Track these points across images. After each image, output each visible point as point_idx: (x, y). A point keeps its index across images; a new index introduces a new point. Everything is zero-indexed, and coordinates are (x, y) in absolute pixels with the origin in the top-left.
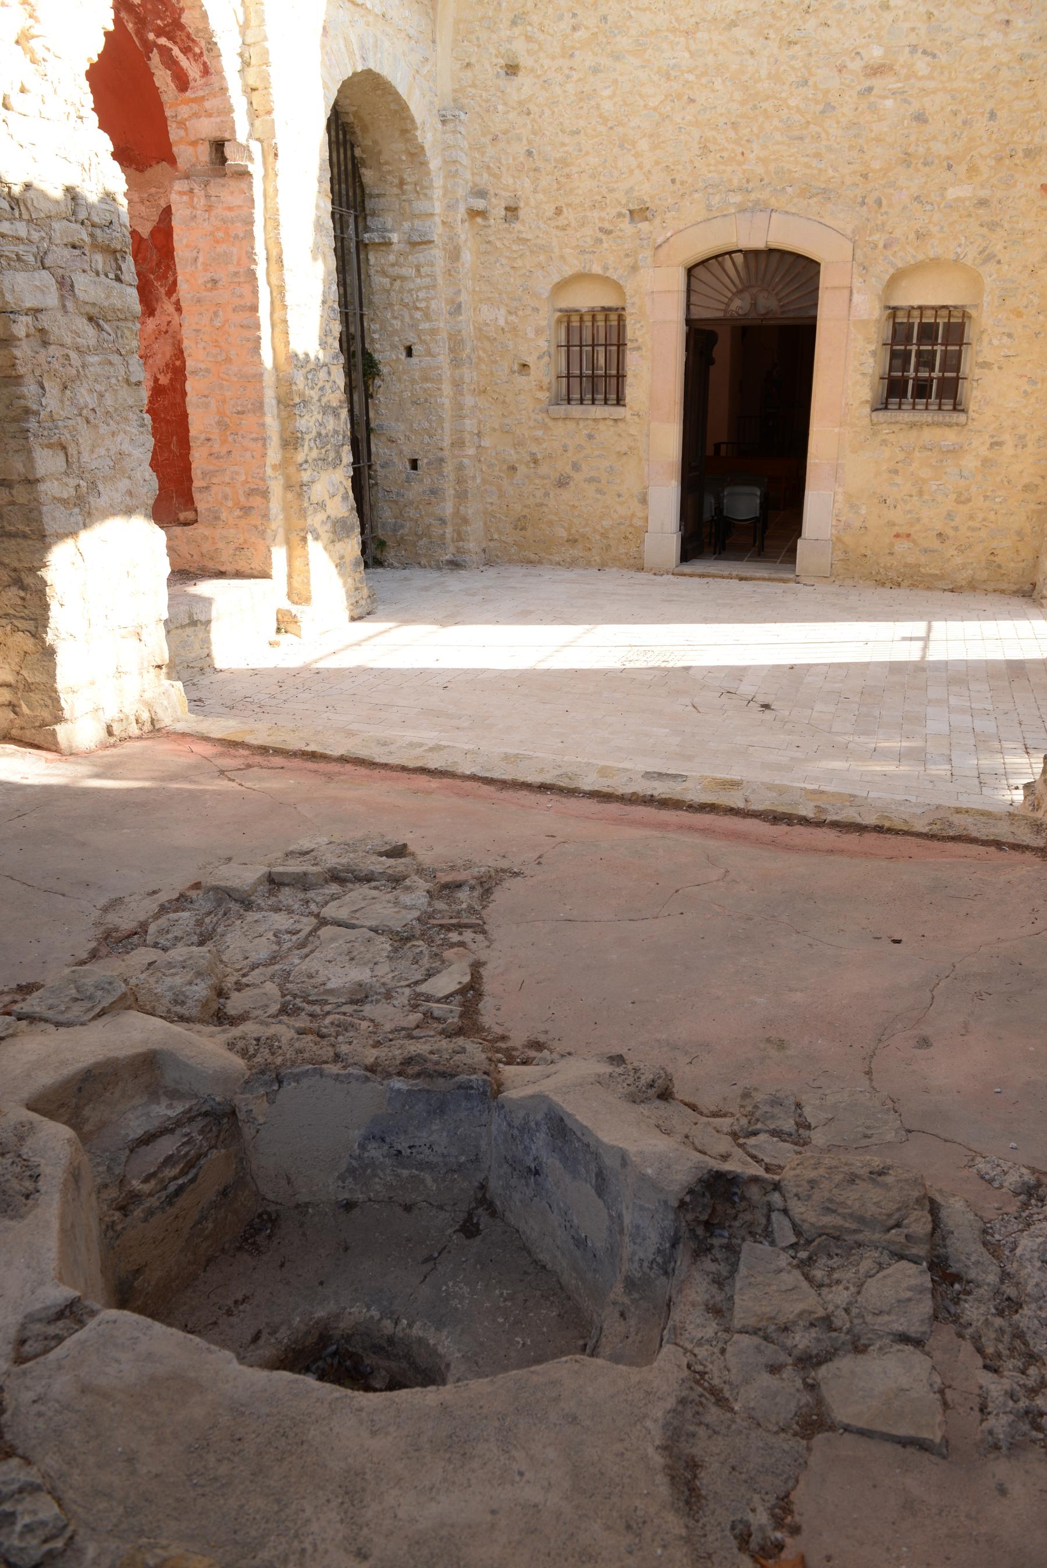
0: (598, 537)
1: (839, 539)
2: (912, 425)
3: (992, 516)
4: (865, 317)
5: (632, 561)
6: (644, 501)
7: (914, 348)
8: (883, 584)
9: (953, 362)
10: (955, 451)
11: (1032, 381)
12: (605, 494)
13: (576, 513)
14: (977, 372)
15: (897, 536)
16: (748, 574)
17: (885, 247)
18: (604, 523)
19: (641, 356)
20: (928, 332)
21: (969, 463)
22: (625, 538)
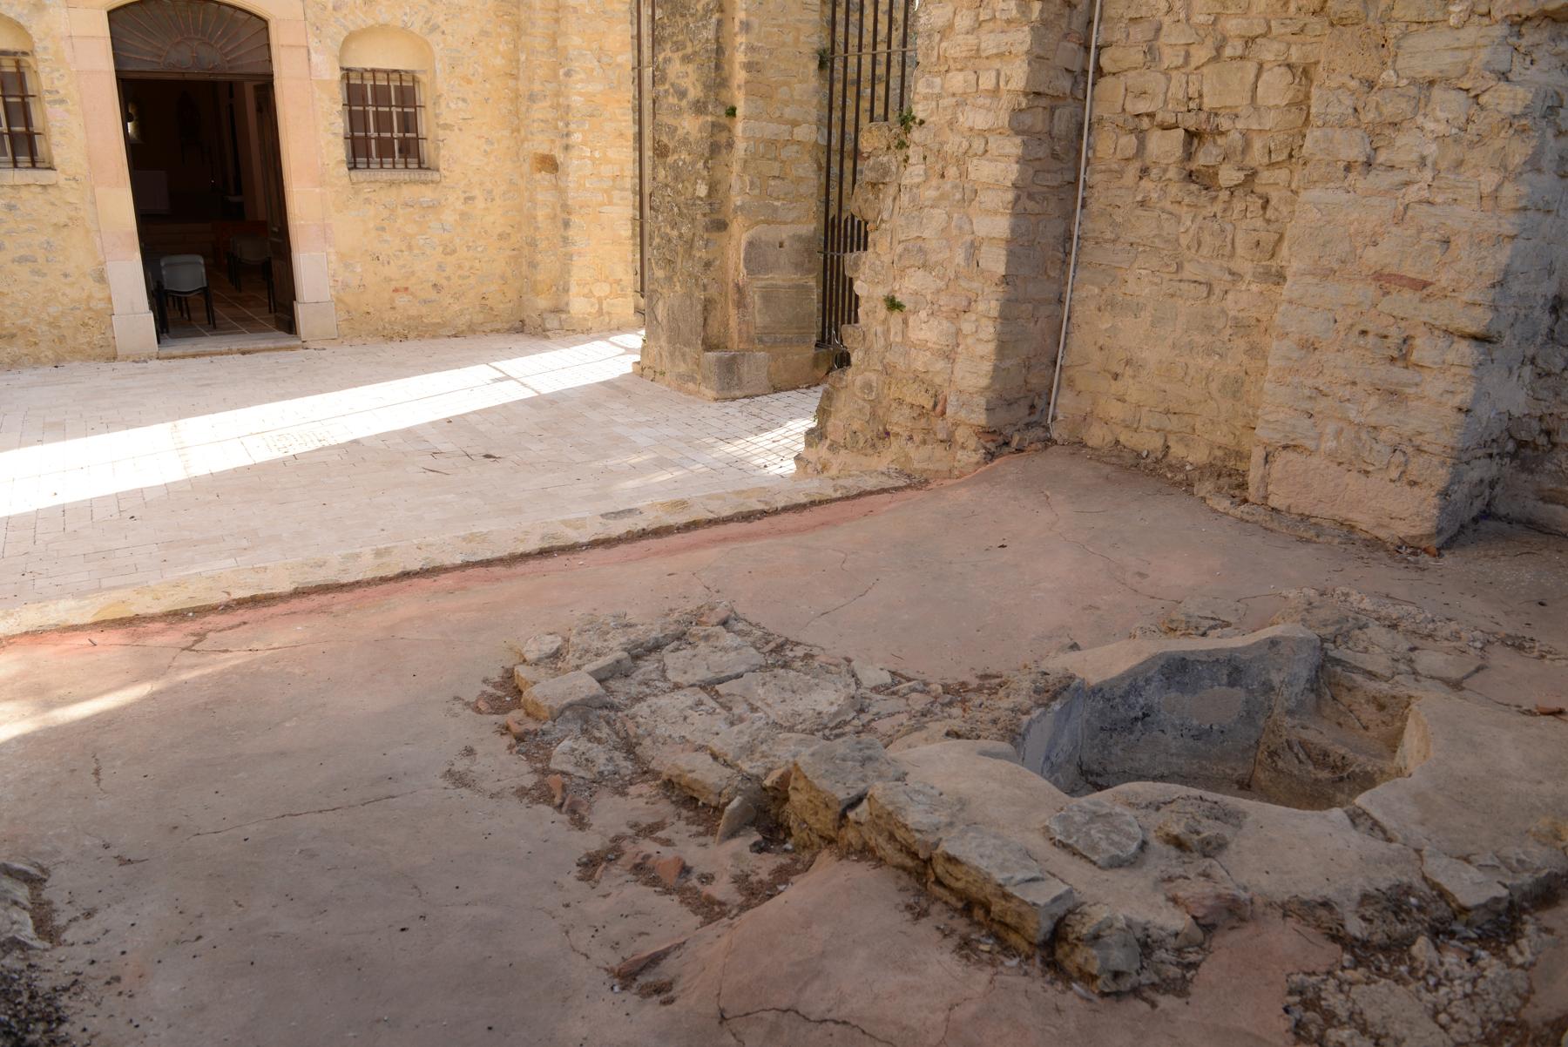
0: (45, 328)
1: (339, 300)
2: (391, 183)
3: (477, 264)
4: (327, 77)
5: (98, 351)
6: (101, 278)
7: (371, 109)
8: (391, 339)
9: (409, 123)
10: (434, 207)
11: (489, 142)
12: (45, 275)
13: (8, 302)
14: (441, 133)
15: (396, 290)
16: (251, 347)
17: (335, 9)
18: (51, 310)
19: (67, 111)
20: (381, 94)
21: (449, 217)
22: (84, 325)
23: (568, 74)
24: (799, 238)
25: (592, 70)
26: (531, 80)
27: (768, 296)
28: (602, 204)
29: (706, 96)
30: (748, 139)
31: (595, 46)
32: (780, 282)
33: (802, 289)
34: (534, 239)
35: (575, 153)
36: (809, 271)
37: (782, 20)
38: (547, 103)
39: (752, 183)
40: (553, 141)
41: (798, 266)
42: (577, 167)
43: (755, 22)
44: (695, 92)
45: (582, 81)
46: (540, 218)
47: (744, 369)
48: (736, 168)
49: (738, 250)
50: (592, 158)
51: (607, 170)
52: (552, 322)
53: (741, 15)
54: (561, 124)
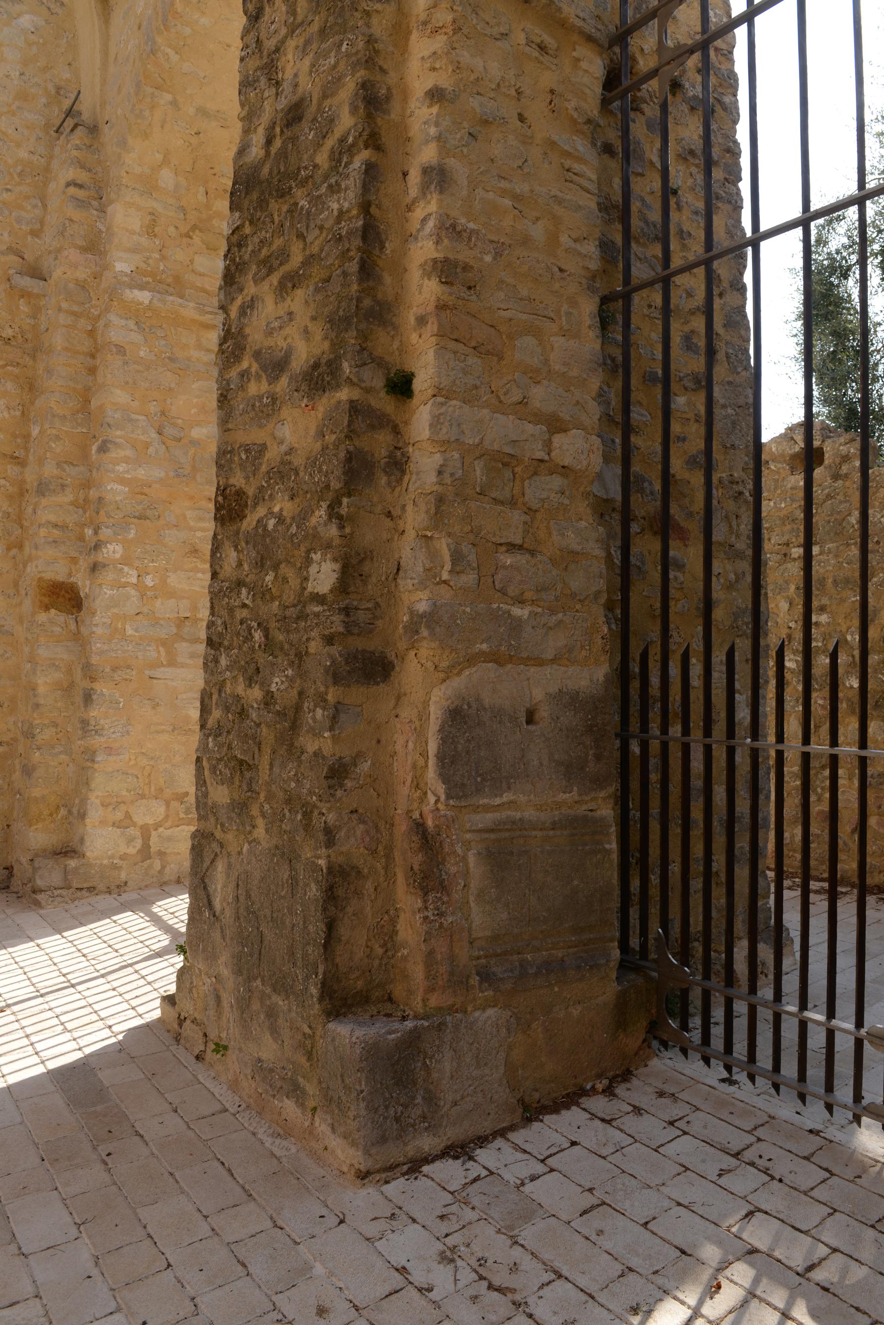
23: (103, 449)
24: (569, 700)
25: (147, 445)
26: (41, 462)
27: (504, 852)
28: (156, 665)
29: (337, 345)
30: (445, 445)
31: (153, 408)
32: (530, 814)
33: (581, 826)
34: (31, 726)
35: (109, 576)
36: (598, 782)
37: (521, 187)
38: (68, 497)
39: (457, 557)
40: (74, 560)
41: (571, 771)
42: (111, 600)
43: (459, 169)
44: (304, 347)
45: (127, 460)
46: (41, 690)
47: (444, 1065)
48: (414, 518)
49: (420, 734)
50: (140, 587)
51: (166, 608)
52: (49, 875)
53: (428, 154)
54: (89, 532)
